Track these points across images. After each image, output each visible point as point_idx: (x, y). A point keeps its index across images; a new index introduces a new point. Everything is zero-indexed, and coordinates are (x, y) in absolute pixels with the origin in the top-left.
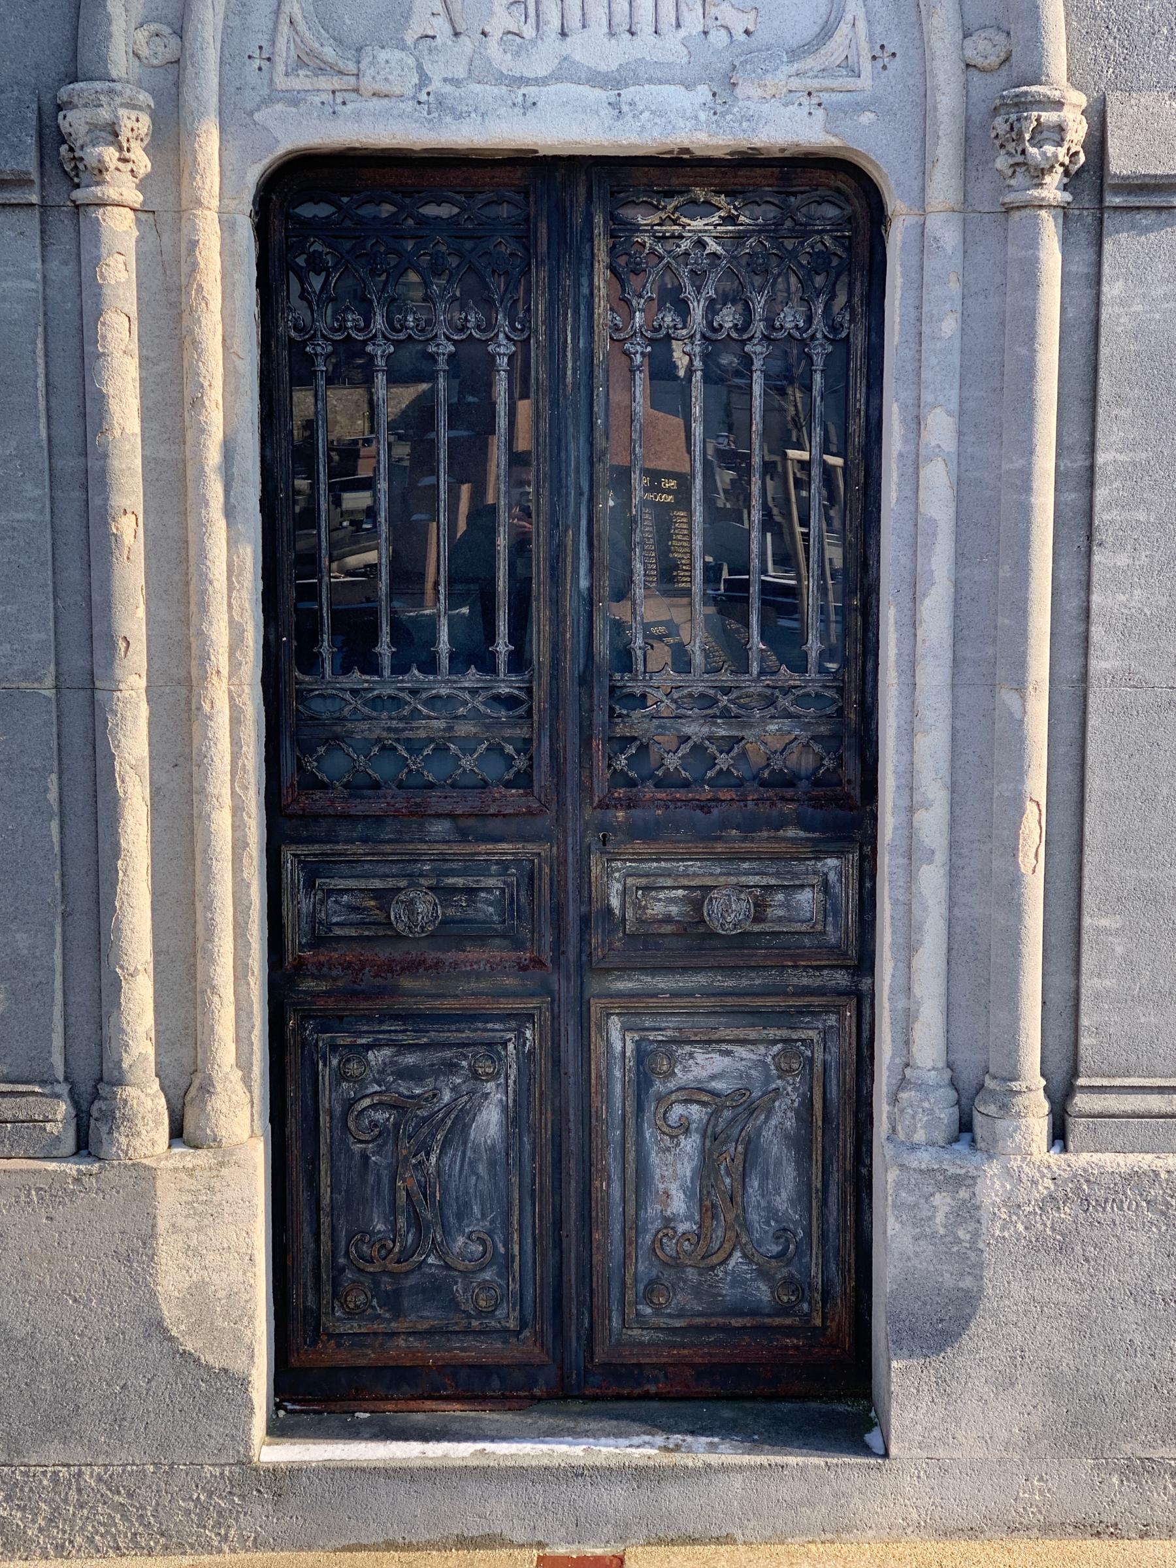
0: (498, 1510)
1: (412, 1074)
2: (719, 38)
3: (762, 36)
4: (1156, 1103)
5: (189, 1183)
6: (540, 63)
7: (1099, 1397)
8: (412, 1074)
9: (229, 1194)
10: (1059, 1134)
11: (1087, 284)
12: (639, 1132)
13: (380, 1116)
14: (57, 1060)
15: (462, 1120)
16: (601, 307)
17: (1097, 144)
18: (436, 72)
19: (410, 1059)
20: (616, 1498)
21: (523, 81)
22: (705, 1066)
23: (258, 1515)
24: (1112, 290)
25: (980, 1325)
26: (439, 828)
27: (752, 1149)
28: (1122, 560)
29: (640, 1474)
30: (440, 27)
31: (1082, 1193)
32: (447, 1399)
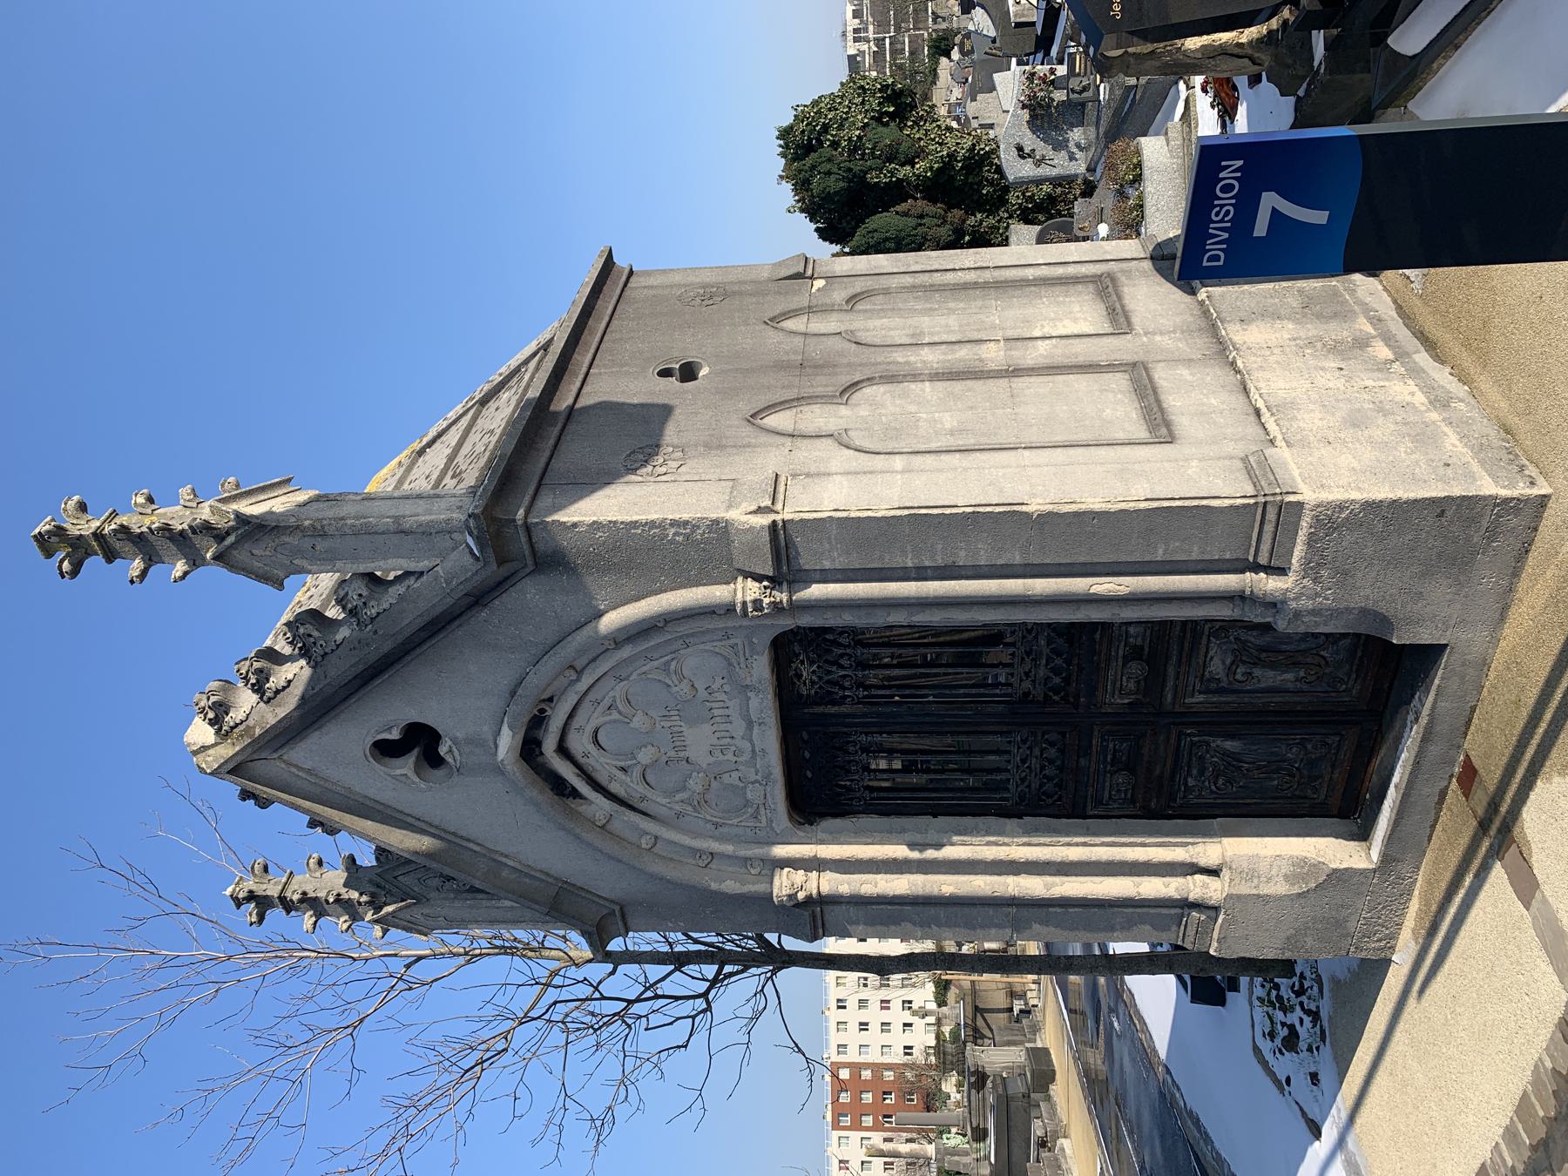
0: (1429, 791)
1: (1202, 772)
2: (727, 688)
3: (725, 673)
4: (1269, 528)
5: (1237, 881)
6: (747, 746)
7: (1439, 555)
8: (1202, 772)
9: (1245, 865)
10: (1282, 571)
11: (826, 577)
12: (1248, 692)
13: (1221, 781)
14: (1173, 911)
15: (1226, 754)
16: (843, 709)
17: (758, 578)
18: (753, 777)
19: (1195, 772)
20: (1434, 750)
21: (753, 751)
22: (1217, 667)
23: (1404, 869)
24: (827, 565)
25: (1382, 608)
26: (1083, 762)
27: (1262, 649)
28: (962, 554)
29: (1426, 739)
30: (735, 775)
31: (1311, 568)
32: (1369, 762)
